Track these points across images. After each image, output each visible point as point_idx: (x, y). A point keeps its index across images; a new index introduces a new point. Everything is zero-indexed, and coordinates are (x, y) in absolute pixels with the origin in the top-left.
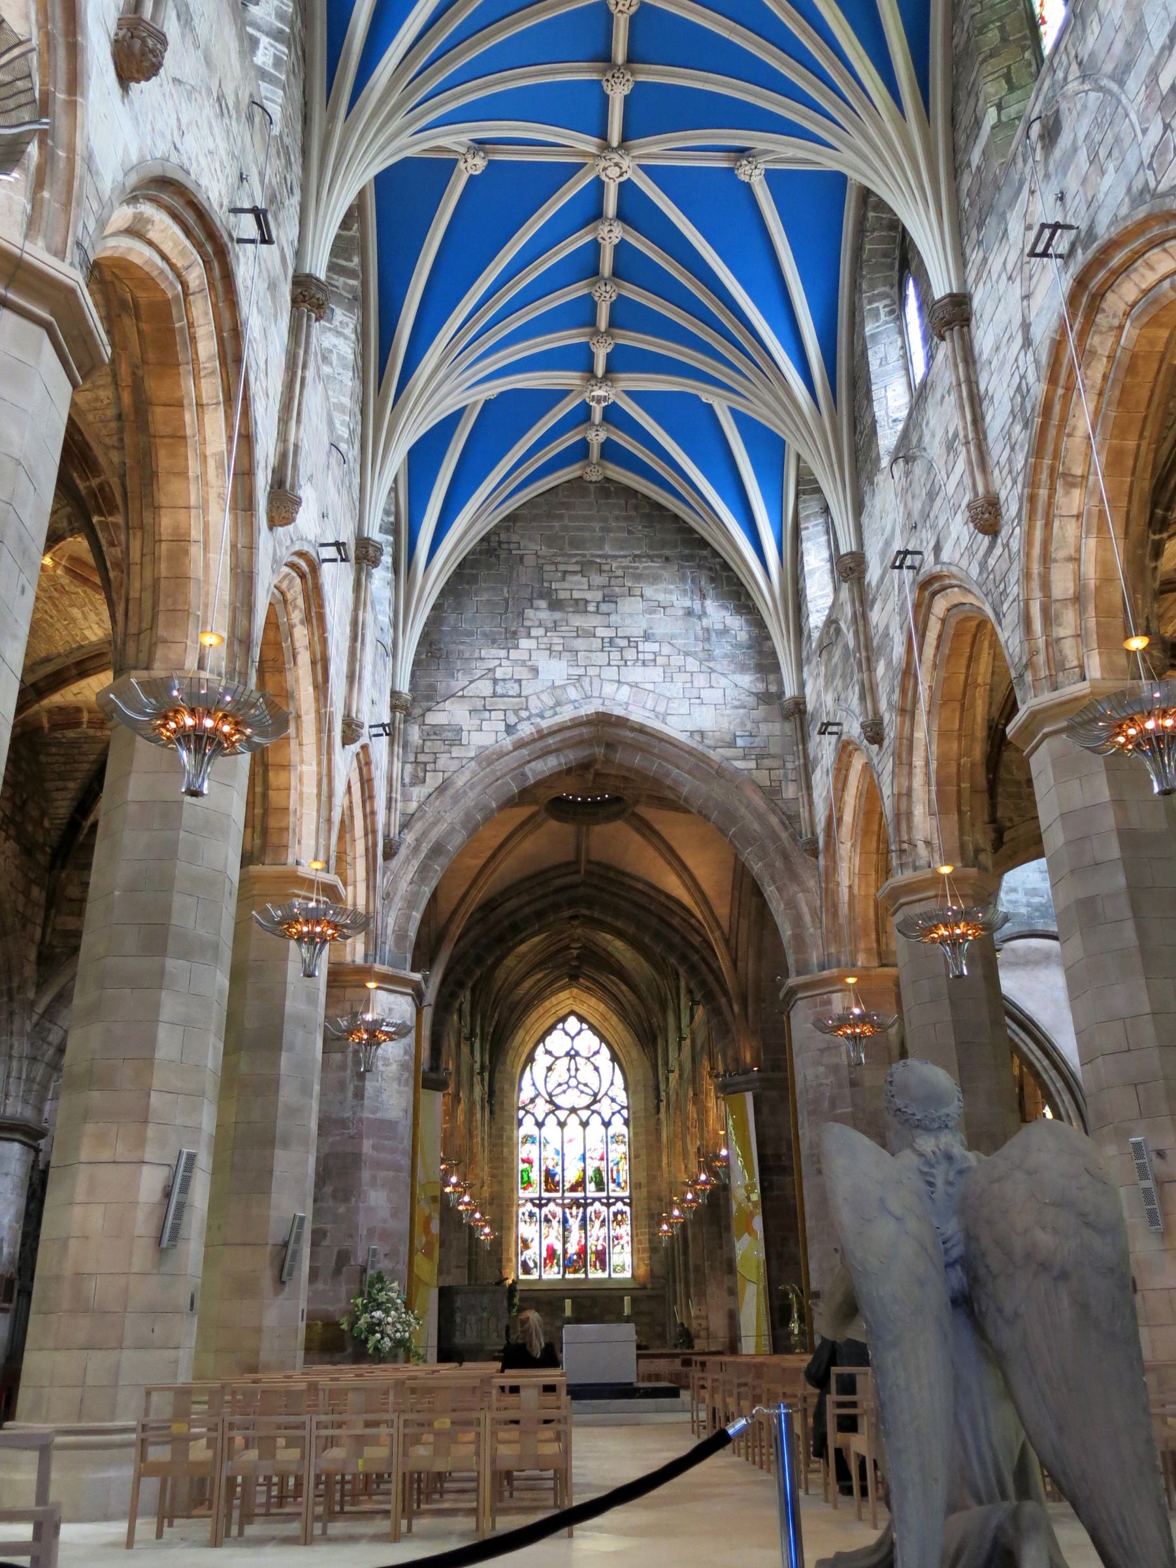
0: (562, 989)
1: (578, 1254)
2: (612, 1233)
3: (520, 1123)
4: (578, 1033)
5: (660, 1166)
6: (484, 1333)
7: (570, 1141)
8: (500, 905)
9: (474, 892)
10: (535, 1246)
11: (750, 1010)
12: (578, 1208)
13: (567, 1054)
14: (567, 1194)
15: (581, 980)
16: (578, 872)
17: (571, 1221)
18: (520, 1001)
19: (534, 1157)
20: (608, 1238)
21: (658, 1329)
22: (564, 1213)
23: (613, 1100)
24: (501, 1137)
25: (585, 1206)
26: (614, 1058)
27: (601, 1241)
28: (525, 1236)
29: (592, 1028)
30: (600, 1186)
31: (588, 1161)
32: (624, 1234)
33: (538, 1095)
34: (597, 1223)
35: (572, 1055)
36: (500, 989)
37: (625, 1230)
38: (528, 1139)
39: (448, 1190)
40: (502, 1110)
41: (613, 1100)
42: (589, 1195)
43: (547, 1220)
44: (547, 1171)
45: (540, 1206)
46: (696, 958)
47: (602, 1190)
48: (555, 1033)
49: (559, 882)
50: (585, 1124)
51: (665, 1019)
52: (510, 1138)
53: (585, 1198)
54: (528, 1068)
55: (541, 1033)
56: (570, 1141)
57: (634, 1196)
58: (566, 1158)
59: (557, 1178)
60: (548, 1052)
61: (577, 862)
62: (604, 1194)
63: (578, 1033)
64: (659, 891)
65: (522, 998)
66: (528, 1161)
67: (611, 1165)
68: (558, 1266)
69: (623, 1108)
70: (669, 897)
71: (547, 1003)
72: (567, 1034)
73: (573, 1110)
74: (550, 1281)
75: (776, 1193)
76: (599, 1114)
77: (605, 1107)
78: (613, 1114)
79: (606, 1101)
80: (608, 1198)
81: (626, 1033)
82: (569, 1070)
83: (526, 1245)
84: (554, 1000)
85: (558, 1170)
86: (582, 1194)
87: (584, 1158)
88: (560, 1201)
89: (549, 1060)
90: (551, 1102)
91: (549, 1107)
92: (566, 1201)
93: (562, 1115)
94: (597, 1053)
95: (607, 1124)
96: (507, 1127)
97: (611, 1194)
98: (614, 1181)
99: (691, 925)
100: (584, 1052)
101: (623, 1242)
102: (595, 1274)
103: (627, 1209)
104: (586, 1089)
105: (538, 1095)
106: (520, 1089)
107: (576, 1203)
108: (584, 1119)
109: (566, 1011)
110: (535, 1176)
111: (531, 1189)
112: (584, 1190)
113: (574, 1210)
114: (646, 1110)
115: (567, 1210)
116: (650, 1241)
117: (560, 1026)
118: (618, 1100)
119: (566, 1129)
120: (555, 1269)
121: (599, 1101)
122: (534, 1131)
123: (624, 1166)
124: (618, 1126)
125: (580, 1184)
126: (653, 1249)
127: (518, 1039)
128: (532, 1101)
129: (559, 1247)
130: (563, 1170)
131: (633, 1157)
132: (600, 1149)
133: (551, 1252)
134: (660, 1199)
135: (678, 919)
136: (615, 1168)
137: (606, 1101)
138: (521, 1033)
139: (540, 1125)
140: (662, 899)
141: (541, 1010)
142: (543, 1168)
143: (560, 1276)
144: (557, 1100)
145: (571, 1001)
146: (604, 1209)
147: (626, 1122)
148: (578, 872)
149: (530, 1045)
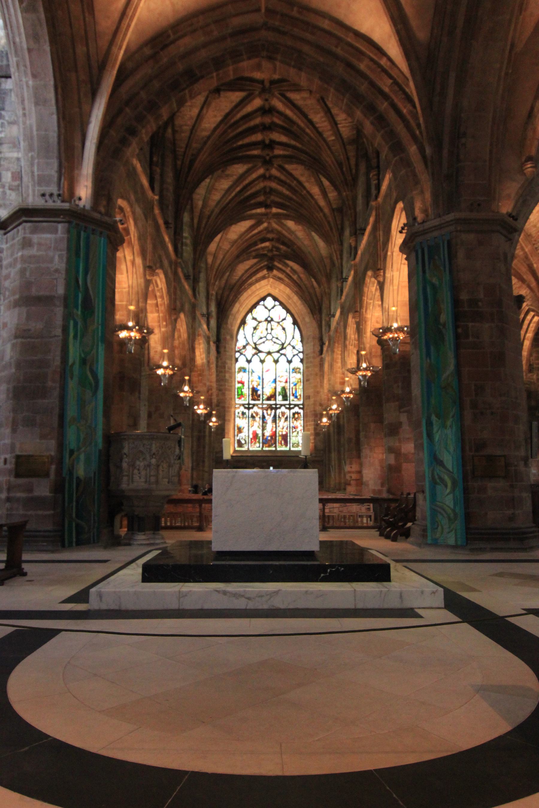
0: (264, 278)
1: (271, 437)
2: (292, 425)
3: (237, 360)
4: (273, 308)
5: (322, 386)
6: (153, 479)
7: (267, 371)
8: (173, 42)
10: (245, 430)
11: (445, 152)
12: (271, 410)
13: (266, 320)
14: (264, 402)
16: (258, 10)
17: (267, 417)
18: (235, 284)
22: (263, 413)
23: (294, 348)
24: (225, 367)
25: (276, 409)
26: (295, 323)
29: (281, 304)
30: (285, 398)
31: (278, 383)
32: (299, 425)
33: (248, 344)
34: (283, 419)
35: (269, 321)
37: (299, 424)
39: (160, 372)
40: (225, 351)
41: (294, 348)
42: (278, 402)
43: (253, 417)
45: (249, 409)
46: (383, 106)
47: (286, 400)
48: (258, 307)
49: (236, 22)
50: (276, 361)
51: (329, 288)
52: (230, 368)
53: (276, 404)
54: (242, 328)
55: (249, 307)
56: (267, 371)
57: (306, 404)
58: (264, 381)
60: (254, 319)
62: (287, 402)
66: (242, 383)
68: (259, 442)
69: (300, 352)
70: (358, 35)
72: (266, 308)
73: (269, 353)
74: (253, 451)
75: (471, 339)
76: (285, 355)
77: (289, 352)
78: (294, 356)
79: (289, 348)
80: (290, 404)
81: (302, 306)
82: (267, 329)
83: (240, 430)
84: (257, 285)
87: (275, 381)
88: (261, 406)
89: (255, 323)
90: (256, 348)
92: (264, 406)
93: (262, 356)
94: (284, 319)
95: (290, 362)
96: (228, 361)
97: (292, 402)
98: (293, 395)
99: (379, 66)
100: (276, 319)
101: (298, 430)
102: (281, 448)
103: (301, 411)
105: (248, 344)
106: (237, 340)
107: (270, 407)
108: (276, 359)
109: (265, 294)
111: (243, 399)
112: (275, 400)
113: (269, 412)
114: (314, 352)
115: (265, 411)
116: (315, 429)
117: (262, 303)
120: (258, 445)
121: (285, 348)
123: (300, 387)
124: (297, 363)
125: (273, 396)
126: (317, 434)
127: (235, 309)
128: (244, 347)
129: (259, 432)
130: (263, 388)
131: (306, 380)
132: (285, 376)
133: (255, 436)
134: (321, 405)
135: (366, 61)
137: (289, 348)
138: (237, 305)
139: (249, 361)
140: (350, 39)
141: (249, 291)
142: (251, 387)
143: (260, 449)
144: (259, 347)
145: (269, 287)
146: (287, 411)
147: (302, 361)
148: (258, 10)
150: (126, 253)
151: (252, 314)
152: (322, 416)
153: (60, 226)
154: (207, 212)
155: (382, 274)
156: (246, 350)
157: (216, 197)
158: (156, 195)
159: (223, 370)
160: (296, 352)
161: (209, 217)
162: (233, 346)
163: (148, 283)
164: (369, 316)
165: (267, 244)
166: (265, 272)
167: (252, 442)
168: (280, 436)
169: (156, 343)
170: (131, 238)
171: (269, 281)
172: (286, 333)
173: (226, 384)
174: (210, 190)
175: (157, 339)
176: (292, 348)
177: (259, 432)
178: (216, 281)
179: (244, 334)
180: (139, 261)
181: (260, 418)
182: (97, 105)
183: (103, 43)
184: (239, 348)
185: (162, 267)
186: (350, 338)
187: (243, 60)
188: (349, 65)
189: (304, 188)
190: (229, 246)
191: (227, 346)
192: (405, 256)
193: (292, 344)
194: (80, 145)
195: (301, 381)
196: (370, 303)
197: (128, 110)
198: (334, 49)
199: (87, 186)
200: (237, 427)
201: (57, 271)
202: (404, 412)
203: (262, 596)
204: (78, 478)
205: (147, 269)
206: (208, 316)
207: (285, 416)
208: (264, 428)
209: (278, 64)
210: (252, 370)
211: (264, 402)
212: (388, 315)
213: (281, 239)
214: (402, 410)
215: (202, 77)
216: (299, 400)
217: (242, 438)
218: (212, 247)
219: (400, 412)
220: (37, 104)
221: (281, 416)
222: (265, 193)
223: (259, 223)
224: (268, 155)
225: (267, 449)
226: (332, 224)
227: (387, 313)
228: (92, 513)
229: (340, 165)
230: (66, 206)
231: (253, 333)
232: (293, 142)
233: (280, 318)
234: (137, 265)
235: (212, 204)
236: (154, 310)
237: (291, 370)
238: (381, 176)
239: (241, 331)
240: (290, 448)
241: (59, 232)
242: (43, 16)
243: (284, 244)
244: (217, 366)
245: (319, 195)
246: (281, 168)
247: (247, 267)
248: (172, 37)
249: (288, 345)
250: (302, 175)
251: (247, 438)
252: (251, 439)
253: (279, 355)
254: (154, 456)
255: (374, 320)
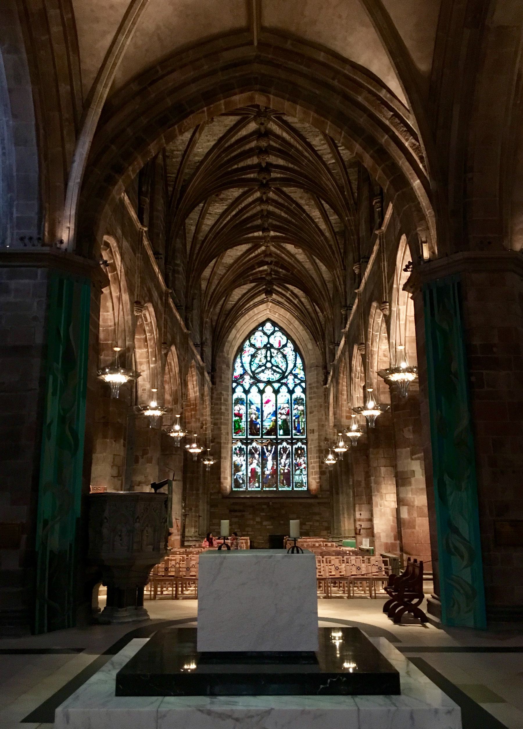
0: (262, 302)
2: (294, 461)
4: (272, 333)
5: (327, 419)
9: (121, 38)
10: (244, 467)
13: (265, 346)
14: (264, 437)
15: (274, 296)
16: (251, 43)
17: (267, 454)
19: (243, 412)
20: (291, 464)
21: (325, 524)
23: (296, 376)
25: (277, 444)
26: (296, 350)
27: (287, 467)
28: (236, 463)
29: (281, 330)
31: (279, 416)
32: (303, 462)
33: (245, 372)
34: (284, 457)
35: (268, 347)
36: (213, 293)
38: (239, 401)
40: (221, 381)
41: (296, 376)
42: (279, 437)
44: (252, 421)
45: (247, 444)
46: (384, 139)
49: (228, 56)
50: (276, 392)
52: (226, 400)
53: (277, 439)
54: (239, 356)
57: (308, 437)
59: (258, 426)
60: (252, 345)
61: (248, 29)
62: (290, 437)
63: (272, 333)
64: (345, 61)
65: (233, 307)
66: (239, 415)
67: (294, 418)
68: (259, 482)
69: (302, 381)
71: (251, 312)
72: (265, 334)
73: (269, 383)
77: (290, 381)
78: (296, 385)
79: (291, 377)
80: (292, 439)
81: (304, 332)
83: (237, 468)
85: (259, 421)
86: (275, 437)
87: (275, 413)
89: (252, 351)
91: (252, 381)
93: (261, 386)
94: (285, 346)
95: (291, 392)
97: (294, 437)
98: (296, 429)
100: (276, 345)
103: (304, 446)
104: (277, 370)
106: (234, 369)
107: (271, 443)
109: (264, 319)
110: (243, 425)
114: (318, 382)
116: (320, 467)
117: (261, 328)
118: (299, 376)
119: (264, 395)
122: (244, 396)
123: (303, 419)
124: (298, 393)
125: (273, 431)
128: (242, 376)
129: (259, 470)
130: (262, 421)
134: (326, 439)
135: (365, 93)
136: (296, 420)
137: (291, 377)
138: (234, 331)
139: (247, 392)
140: (347, 70)
142: (249, 420)
143: (259, 489)
146: (289, 446)
147: (304, 391)
149: (240, 341)
150: (112, 289)
151: (250, 341)
152: (327, 453)
153: (39, 271)
154: (201, 237)
155: (388, 307)
156: (243, 380)
157: (209, 222)
158: (145, 226)
159: (218, 402)
160: (298, 381)
161: (203, 242)
162: (230, 376)
163: (135, 319)
164: (375, 349)
165: (265, 267)
166: (263, 296)
167: (250, 483)
168: (281, 474)
169: (144, 380)
170: (117, 274)
171: (267, 306)
172: (287, 361)
173: (222, 417)
174: (202, 215)
175: (145, 376)
176: (293, 377)
177: (259, 470)
178: (210, 308)
179: (242, 362)
180: (126, 297)
181: (259, 454)
182: (81, 143)
183: (88, 82)
184: (236, 377)
185: (151, 300)
186: (356, 370)
187: (235, 94)
188: (346, 97)
189: (304, 211)
190: (224, 271)
191: (223, 376)
192: (411, 295)
193: (293, 372)
194: (63, 186)
195: (303, 414)
196: (376, 335)
197: (113, 147)
198: (330, 81)
199: (69, 228)
200: (234, 464)
201: (35, 318)
202: (416, 459)
203: (252, 717)
204: (51, 552)
205: (135, 305)
206: (201, 346)
207: (287, 452)
208: (263, 466)
209: (271, 96)
210: (250, 401)
211: (264, 437)
212: (396, 351)
213: (280, 263)
214: (413, 457)
215: (192, 112)
216: (302, 434)
217: (240, 477)
218: (207, 273)
219: (412, 459)
220: (16, 144)
221: (282, 452)
222: (262, 217)
223: (256, 247)
224: (264, 178)
225: (267, 489)
226: (334, 248)
227: (394, 349)
228: (66, 593)
229: (341, 189)
230: (46, 249)
231: (251, 361)
232: (290, 165)
233: (280, 345)
234: (124, 302)
235: (205, 228)
236: (143, 345)
237: (293, 401)
238: (384, 204)
239: (238, 360)
240: (293, 488)
241: (39, 277)
242: (25, 56)
243: (283, 267)
244: (212, 398)
245: (319, 218)
246: (279, 192)
247: (244, 291)
248: (161, 73)
249: (289, 374)
250: (301, 198)
251: (245, 477)
252: (249, 478)
253: (280, 385)
254: (138, 520)
255: (381, 353)
